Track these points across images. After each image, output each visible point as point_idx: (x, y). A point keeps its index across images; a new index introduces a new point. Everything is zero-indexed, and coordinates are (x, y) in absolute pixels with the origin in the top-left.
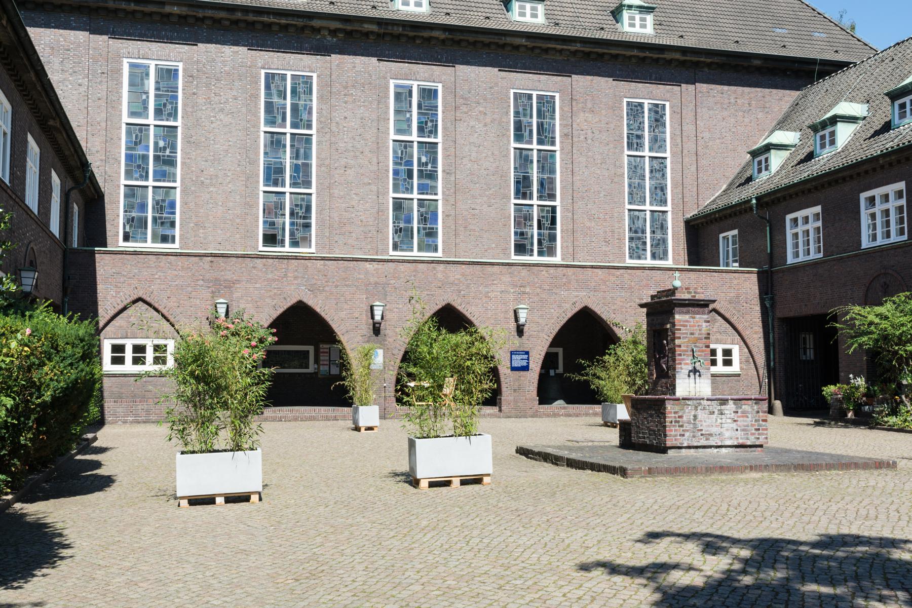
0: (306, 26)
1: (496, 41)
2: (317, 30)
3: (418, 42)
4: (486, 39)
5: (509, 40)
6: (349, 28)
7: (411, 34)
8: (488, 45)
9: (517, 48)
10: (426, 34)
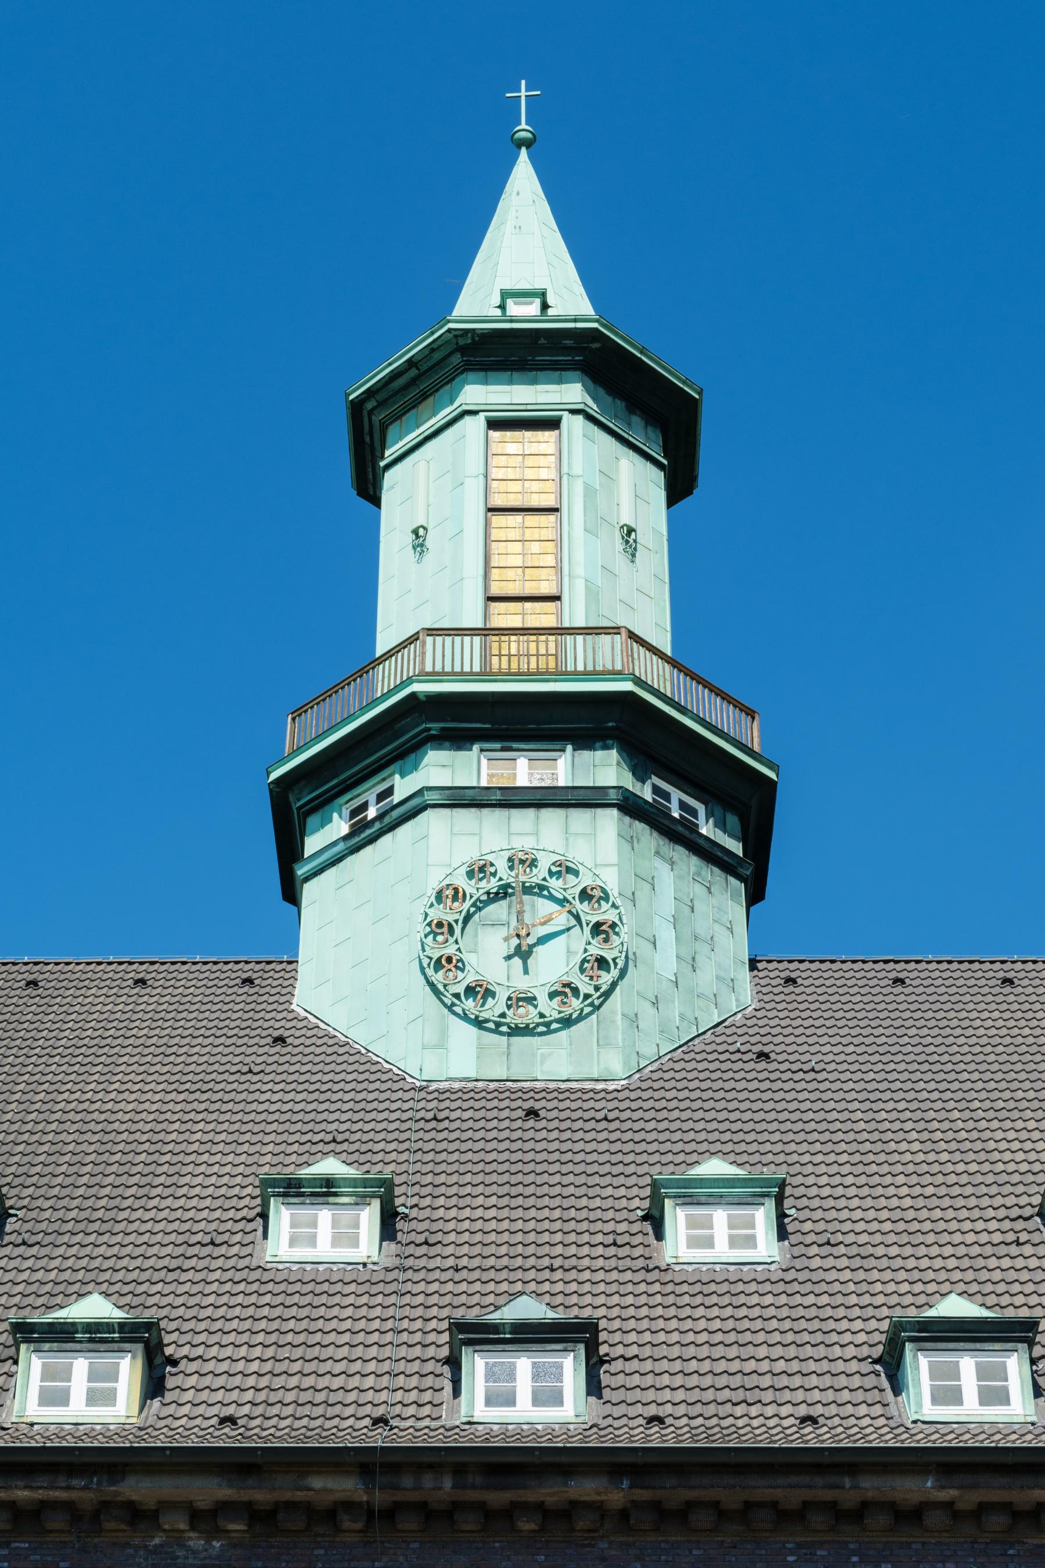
0: (105, 1506)
1: (828, 1495)
2: (139, 1516)
3: (527, 1525)
4: (789, 1493)
5: (871, 1486)
6: (261, 1496)
7: (497, 1498)
8: (799, 1515)
9: (910, 1516)
10: (550, 1492)
